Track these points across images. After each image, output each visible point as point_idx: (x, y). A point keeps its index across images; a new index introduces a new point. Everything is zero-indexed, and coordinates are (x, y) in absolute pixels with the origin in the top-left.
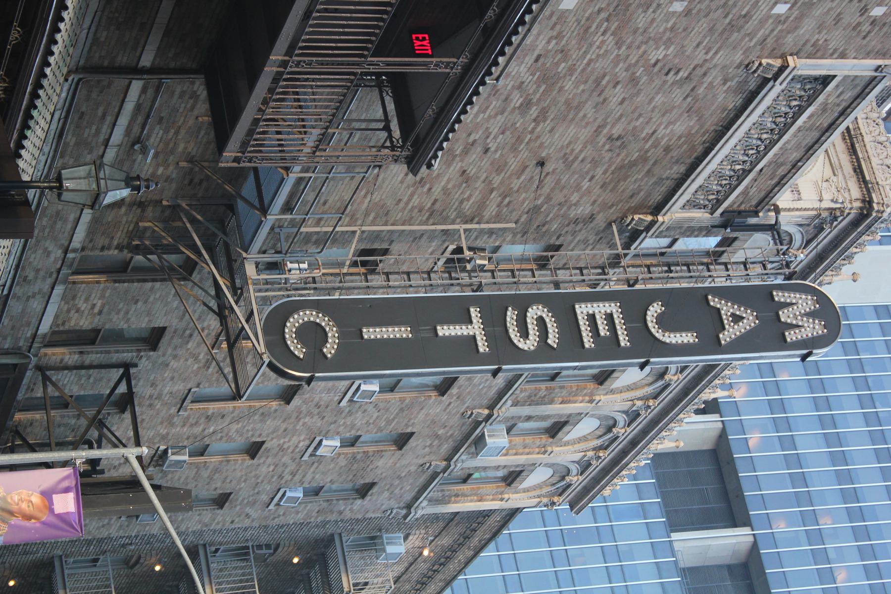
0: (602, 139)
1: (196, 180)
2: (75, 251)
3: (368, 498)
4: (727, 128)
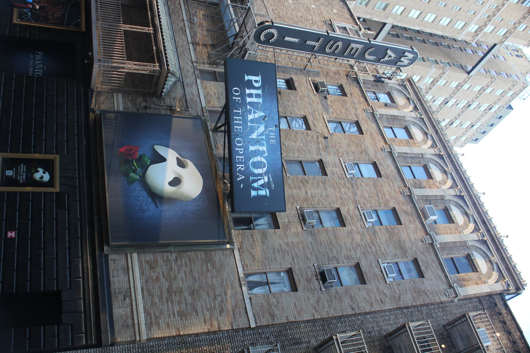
2: (195, 62)
3: (425, 275)
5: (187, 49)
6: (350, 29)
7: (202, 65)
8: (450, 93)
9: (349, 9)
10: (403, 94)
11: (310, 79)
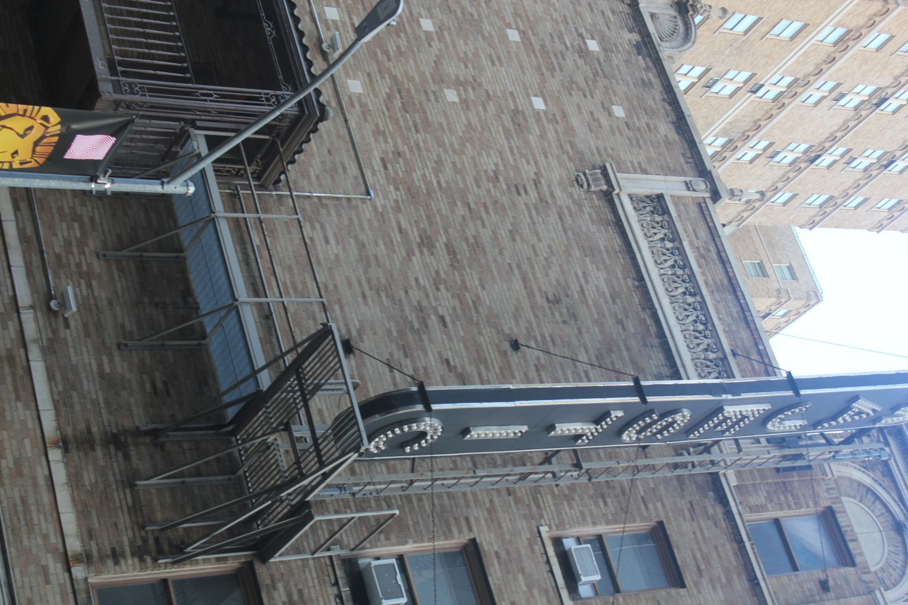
0: (540, 300)
1: (160, 385)
2: (78, 559)
4: (641, 279)
5: (42, 482)
6: (677, 200)
7: (110, 563)
8: (897, 72)
9: (669, 89)
10: (878, 506)
11: (544, 530)
